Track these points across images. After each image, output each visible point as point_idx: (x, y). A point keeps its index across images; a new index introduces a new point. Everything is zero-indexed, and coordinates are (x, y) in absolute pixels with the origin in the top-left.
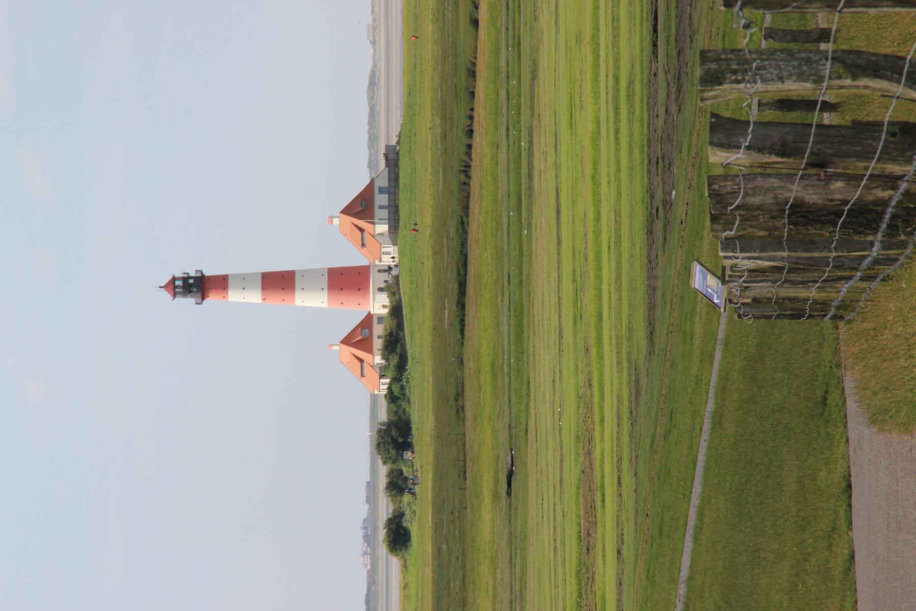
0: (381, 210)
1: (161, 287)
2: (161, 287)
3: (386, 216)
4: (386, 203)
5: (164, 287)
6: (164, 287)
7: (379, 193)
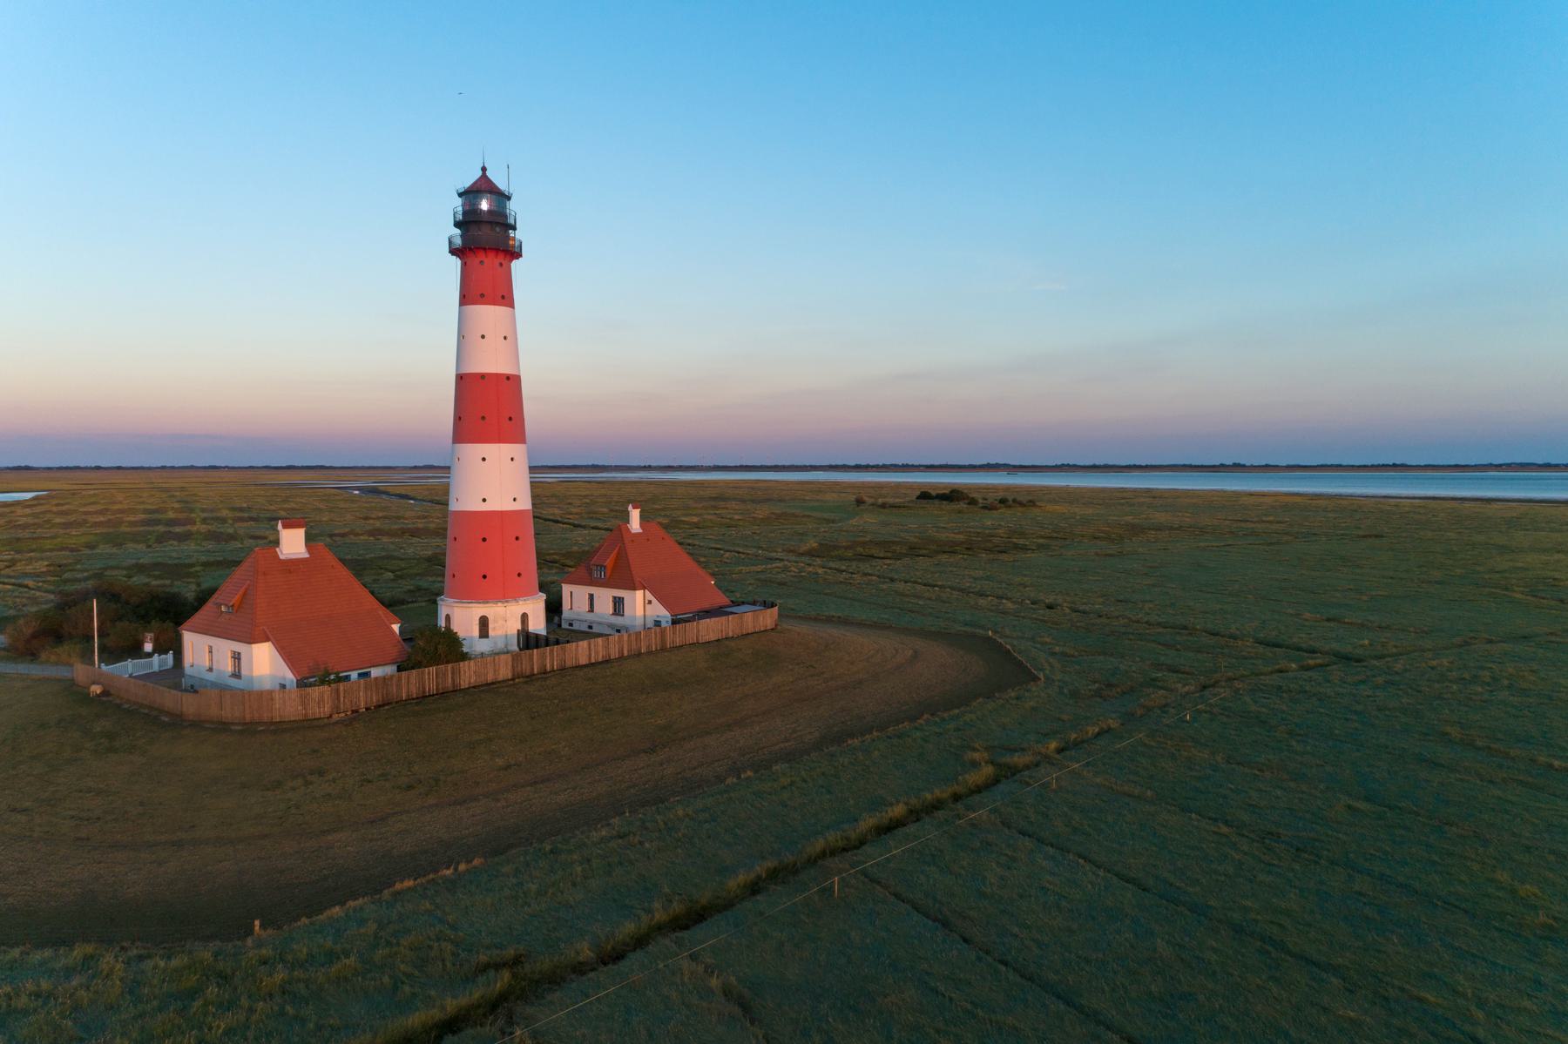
1: (484, 169)
2: (484, 169)
5: (484, 176)
6: (484, 176)
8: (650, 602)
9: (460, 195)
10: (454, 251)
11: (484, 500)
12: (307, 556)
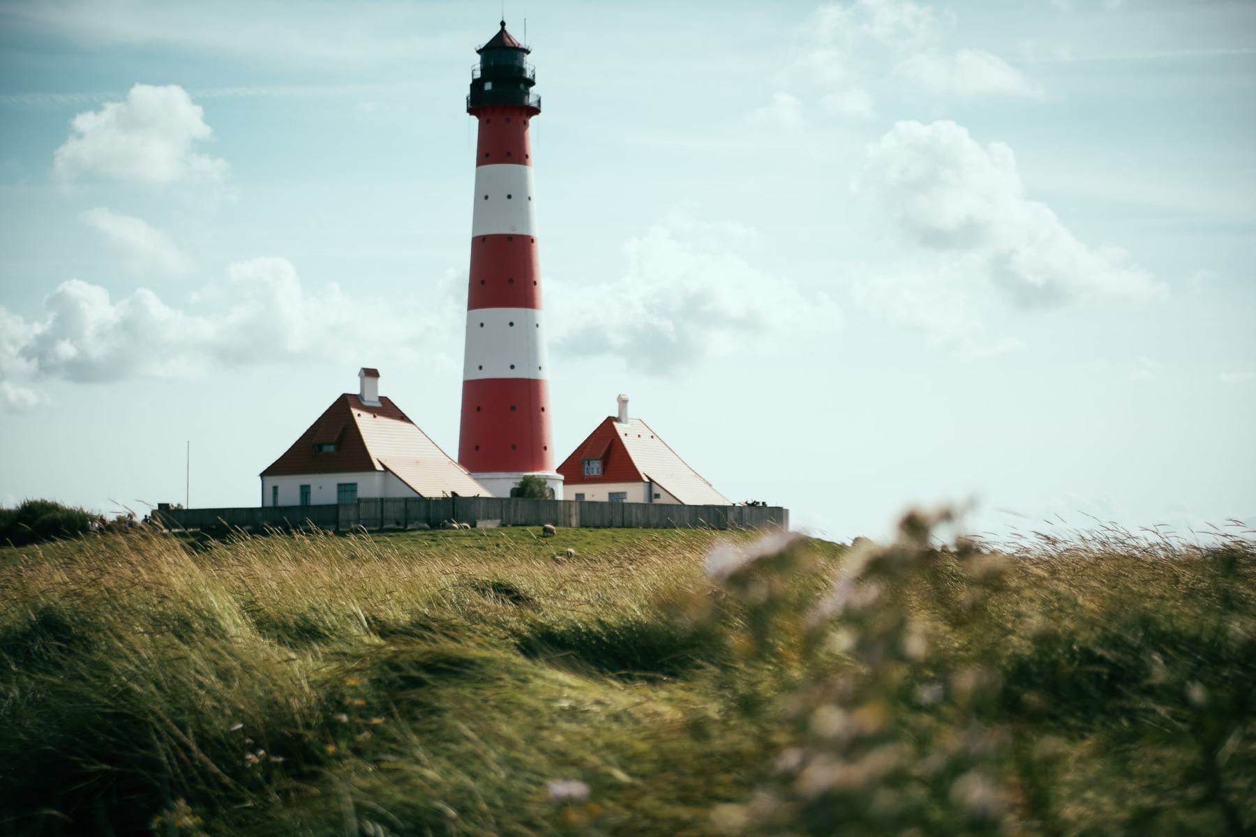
0: (297, 491)
1: (503, 24)
2: (503, 24)
3: (283, 501)
4: (316, 498)
5: (503, 31)
6: (503, 31)
7: (339, 485)
8: (657, 496)
9: (479, 52)
10: (471, 111)
11: (512, 367)
12: (381, 406)
